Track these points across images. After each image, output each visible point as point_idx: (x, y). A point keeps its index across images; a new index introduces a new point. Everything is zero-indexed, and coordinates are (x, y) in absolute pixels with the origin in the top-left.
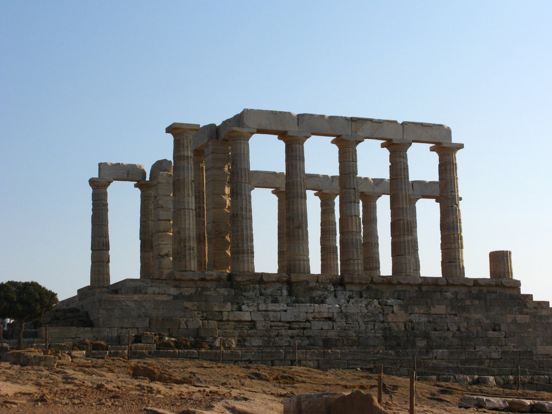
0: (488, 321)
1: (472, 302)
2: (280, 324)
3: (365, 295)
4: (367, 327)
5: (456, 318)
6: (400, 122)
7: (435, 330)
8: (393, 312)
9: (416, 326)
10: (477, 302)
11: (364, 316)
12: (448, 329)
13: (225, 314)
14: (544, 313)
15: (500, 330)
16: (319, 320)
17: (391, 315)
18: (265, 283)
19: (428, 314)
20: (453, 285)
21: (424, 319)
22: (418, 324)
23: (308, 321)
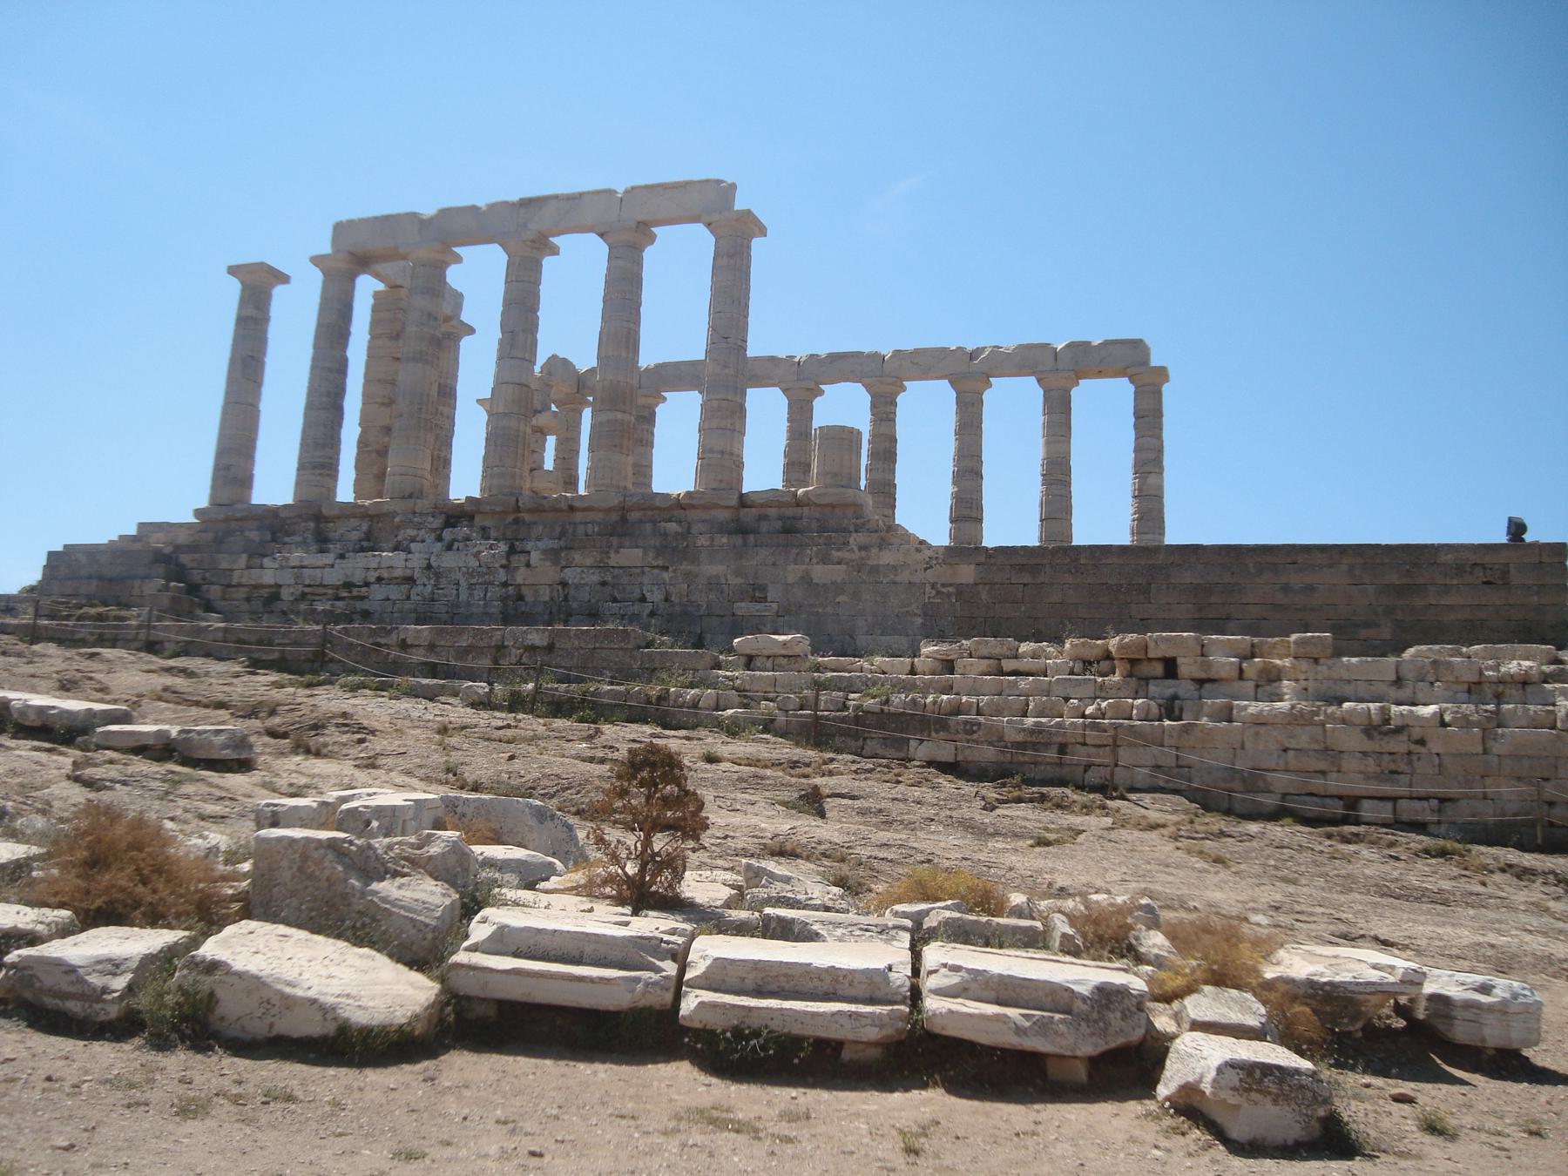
0: (739, 581)
1: (712, 539)
2: (320, 590)
3: (493, 534)
4: (471, 595)
5: (666, 576)
6: (620, 190)
7: (615, 600)
8: (528, 565)
9: (572, 592)
10: (724, 540)
11: (470, 574)
12: (643, 599)
13: (236, 574)
14: (887, 558)
15: (764, 600)
16: (391, 581)
17: (523, 570)
18: (327, 520)
19: (602, 567)
20: (693, 507)
21: (594, 578)
22: (578, 587)
23: (367, 584)
